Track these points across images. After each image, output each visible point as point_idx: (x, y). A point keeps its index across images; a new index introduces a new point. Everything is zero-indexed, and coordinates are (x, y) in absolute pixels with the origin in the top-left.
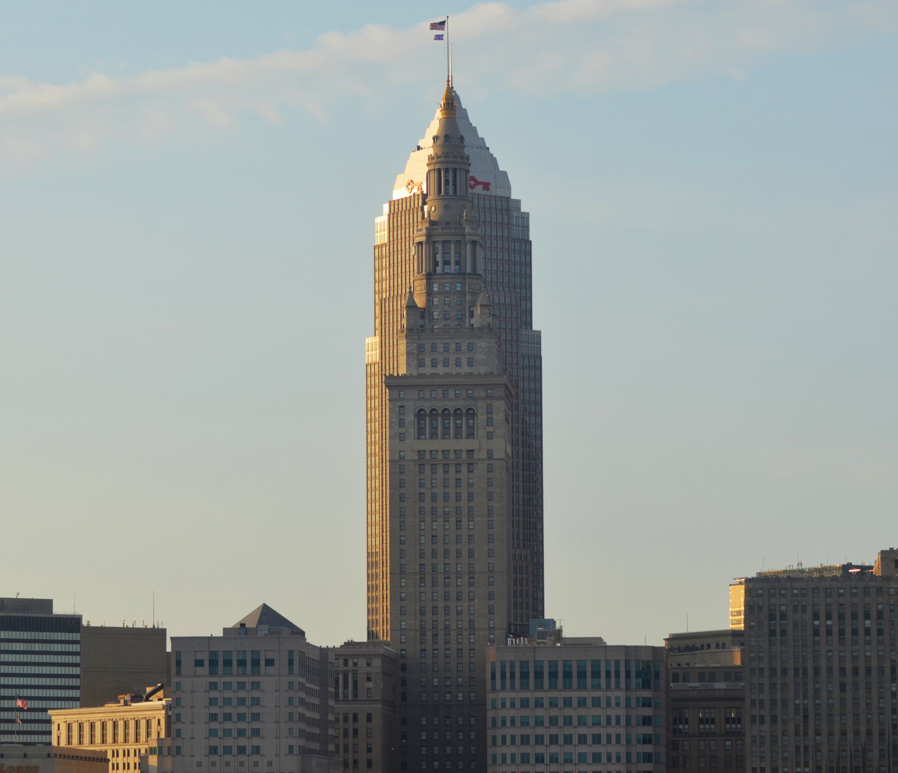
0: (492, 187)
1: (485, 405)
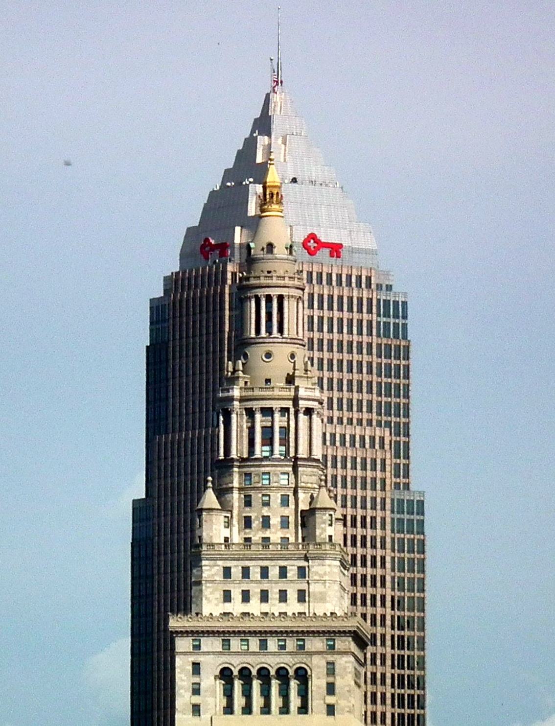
0: (344, 253)
1: (323, 663)
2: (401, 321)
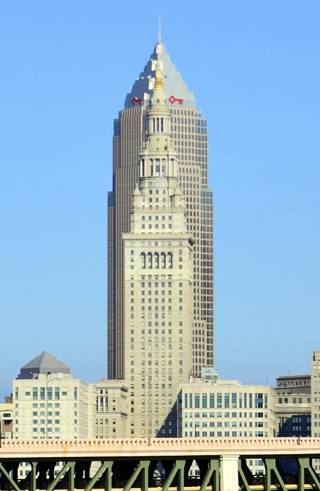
0: (183, 102)
2: (204, 127)
